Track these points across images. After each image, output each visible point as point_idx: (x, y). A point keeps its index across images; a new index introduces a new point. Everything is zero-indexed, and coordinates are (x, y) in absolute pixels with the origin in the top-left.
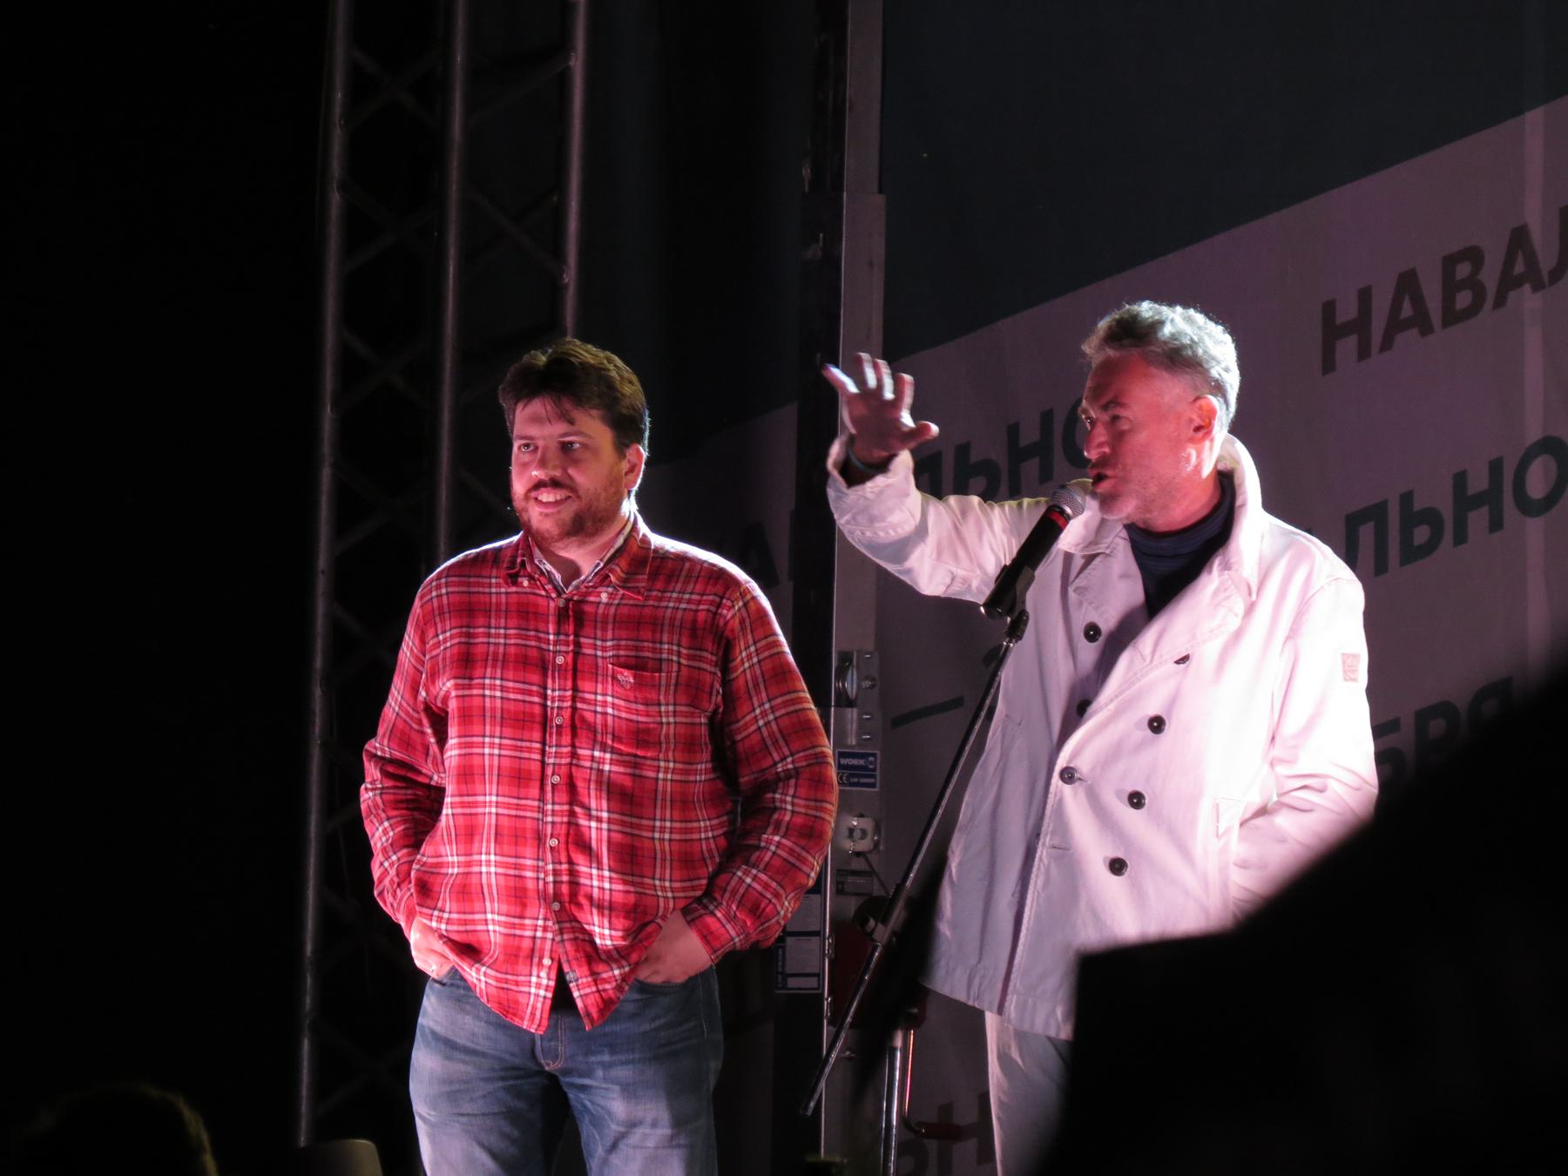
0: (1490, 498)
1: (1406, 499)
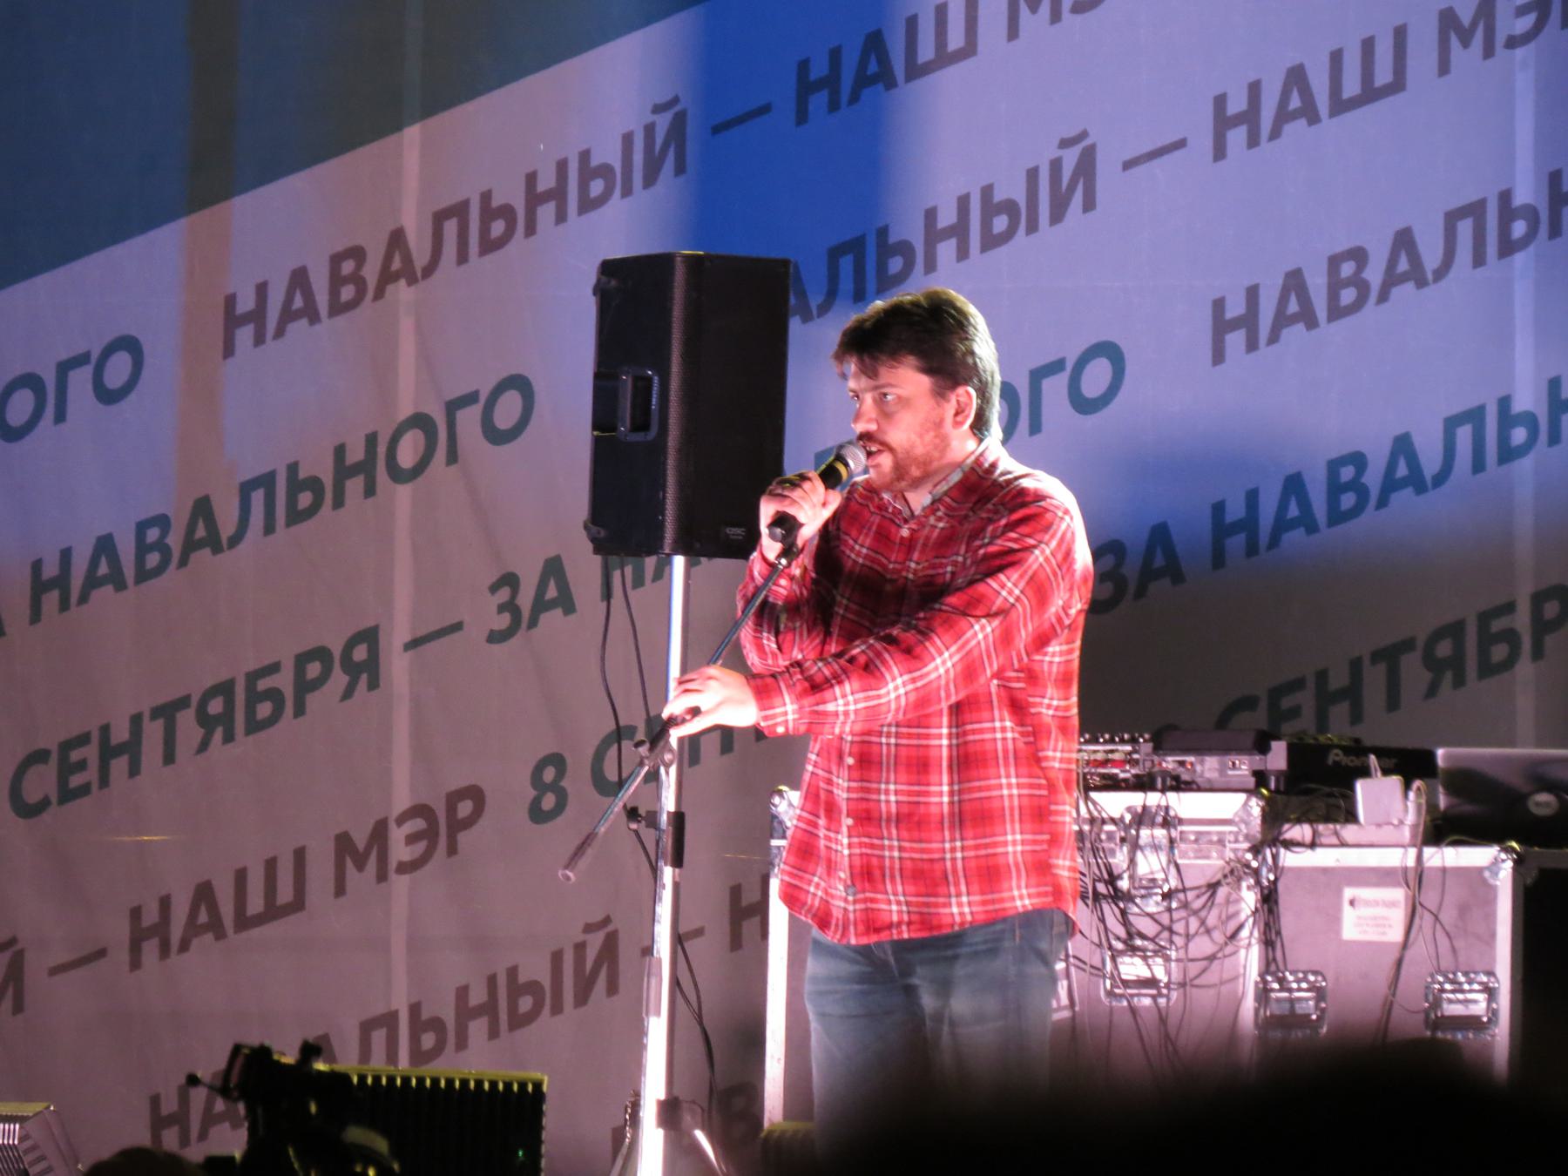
0: (366, 468)
1: (293, 468)
